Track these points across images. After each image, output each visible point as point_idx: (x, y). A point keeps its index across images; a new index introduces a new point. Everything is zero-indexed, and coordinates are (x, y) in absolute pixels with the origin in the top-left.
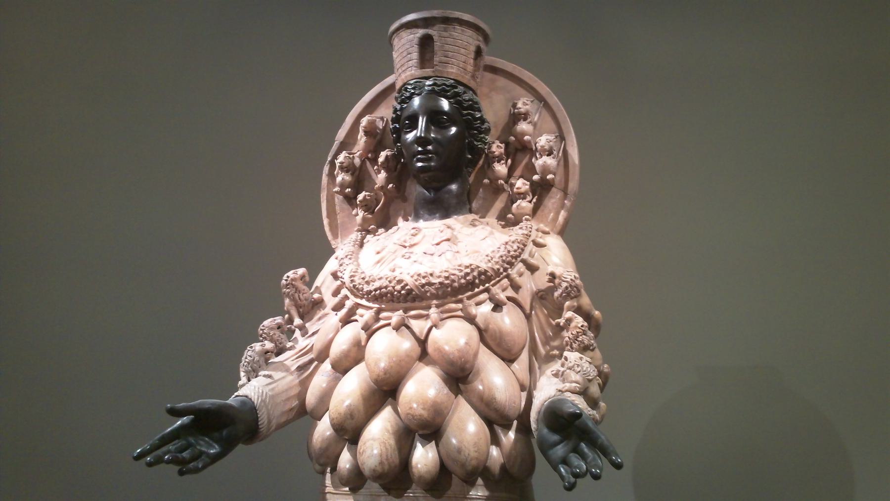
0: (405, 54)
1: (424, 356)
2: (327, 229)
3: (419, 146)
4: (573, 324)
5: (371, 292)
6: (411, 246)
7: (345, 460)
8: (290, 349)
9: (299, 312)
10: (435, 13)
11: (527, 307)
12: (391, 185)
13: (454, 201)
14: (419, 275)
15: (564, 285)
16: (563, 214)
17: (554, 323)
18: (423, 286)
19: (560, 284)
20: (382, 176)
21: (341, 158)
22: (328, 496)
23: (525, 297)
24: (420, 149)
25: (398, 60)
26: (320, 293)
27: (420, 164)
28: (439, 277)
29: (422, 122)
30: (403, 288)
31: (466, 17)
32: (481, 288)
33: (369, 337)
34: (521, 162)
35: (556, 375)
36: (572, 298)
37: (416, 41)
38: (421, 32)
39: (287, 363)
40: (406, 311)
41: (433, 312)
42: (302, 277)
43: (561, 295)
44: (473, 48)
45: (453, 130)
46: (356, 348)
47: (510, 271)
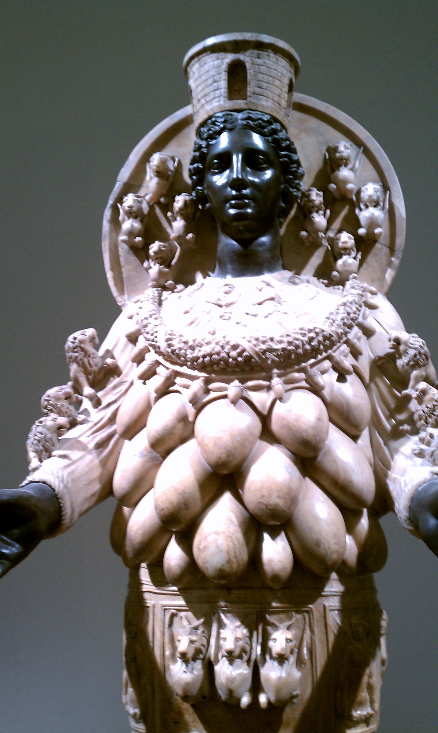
0: (210, 81)
1: (267, 434)
2: (111, 283)
3: (232, 188)
4: (427, 397)
5: (198, 358)
6: (228, 305)
7: (174, 555)
8: (82, 423)
9: (88, 379)
10: (248, 36)
11: (367, 376)
12: (190, 236)
13: (267, 255)
14: (257, 339)
15: (412, 352)
16: (389, 274)
17: (399, 394)
18: (264, 352)
19: (406, 352)
20: (179, 224)
21: (129, 200)
22: (146, 596)
23: (364, 365)
24: (234, 192)
25: (200, 88)
26: (113, 357)
27: (232, 211)
28: (281, 342)
29: (237, 160)
30: (240, 355)
31: (282, 44)
32: (324, 354)
33: (199, 411)
34: (338, 214)
35: (420, 454)
36: (420, 367)
37: (224, 67)
38: (230, 57)
39: (83, 439)
40: (242, 381)
41: (277, 382)
42: (92, 339)
43: (408, 364)
44: (286, 81)
45: (268, 174)
46: (180, 426)
47: (351, 336)
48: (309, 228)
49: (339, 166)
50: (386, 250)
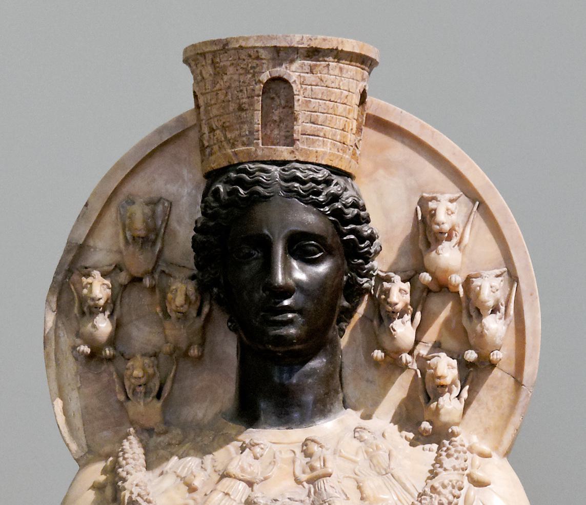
34: (436, 315)
48: (387, 344)
49: (438, 241)
50: (509, 382)
